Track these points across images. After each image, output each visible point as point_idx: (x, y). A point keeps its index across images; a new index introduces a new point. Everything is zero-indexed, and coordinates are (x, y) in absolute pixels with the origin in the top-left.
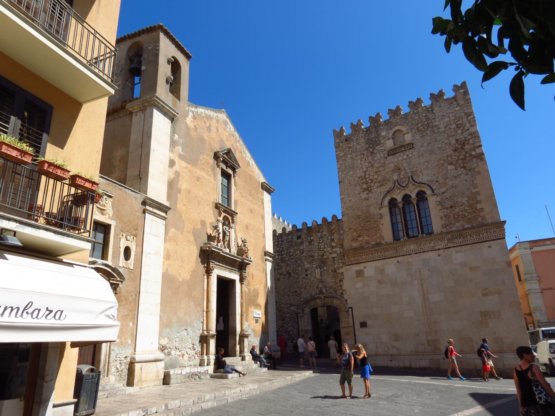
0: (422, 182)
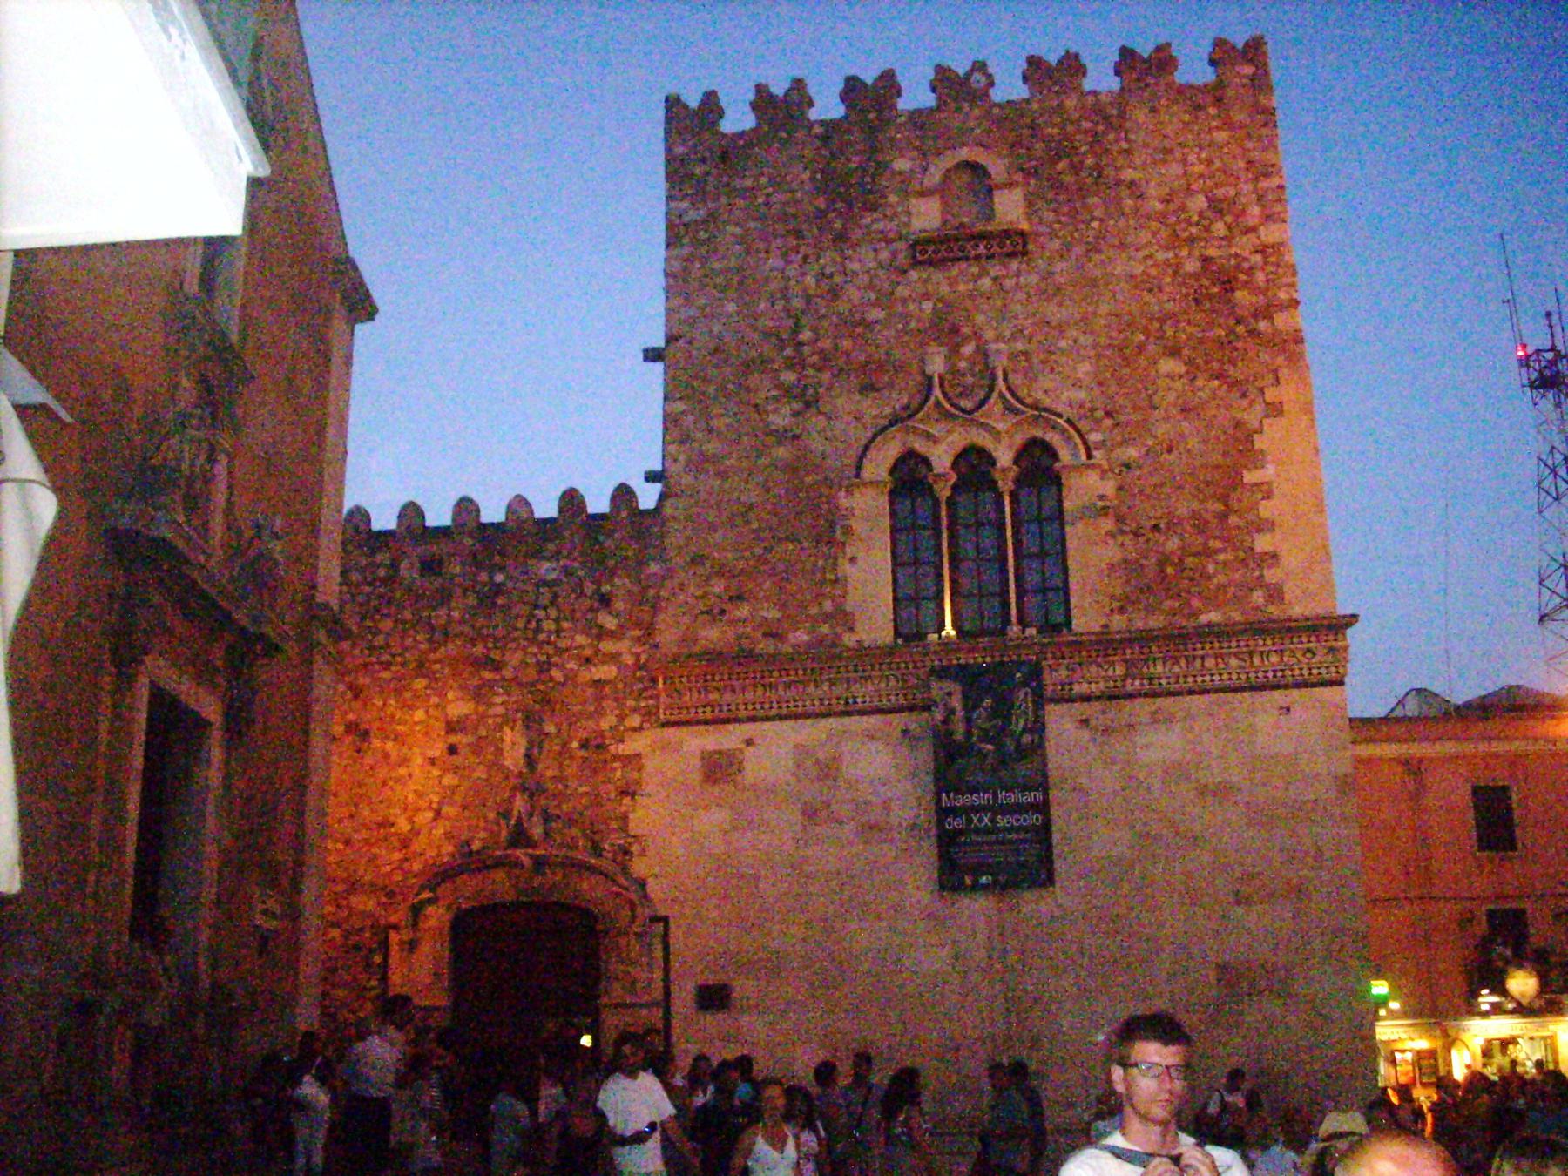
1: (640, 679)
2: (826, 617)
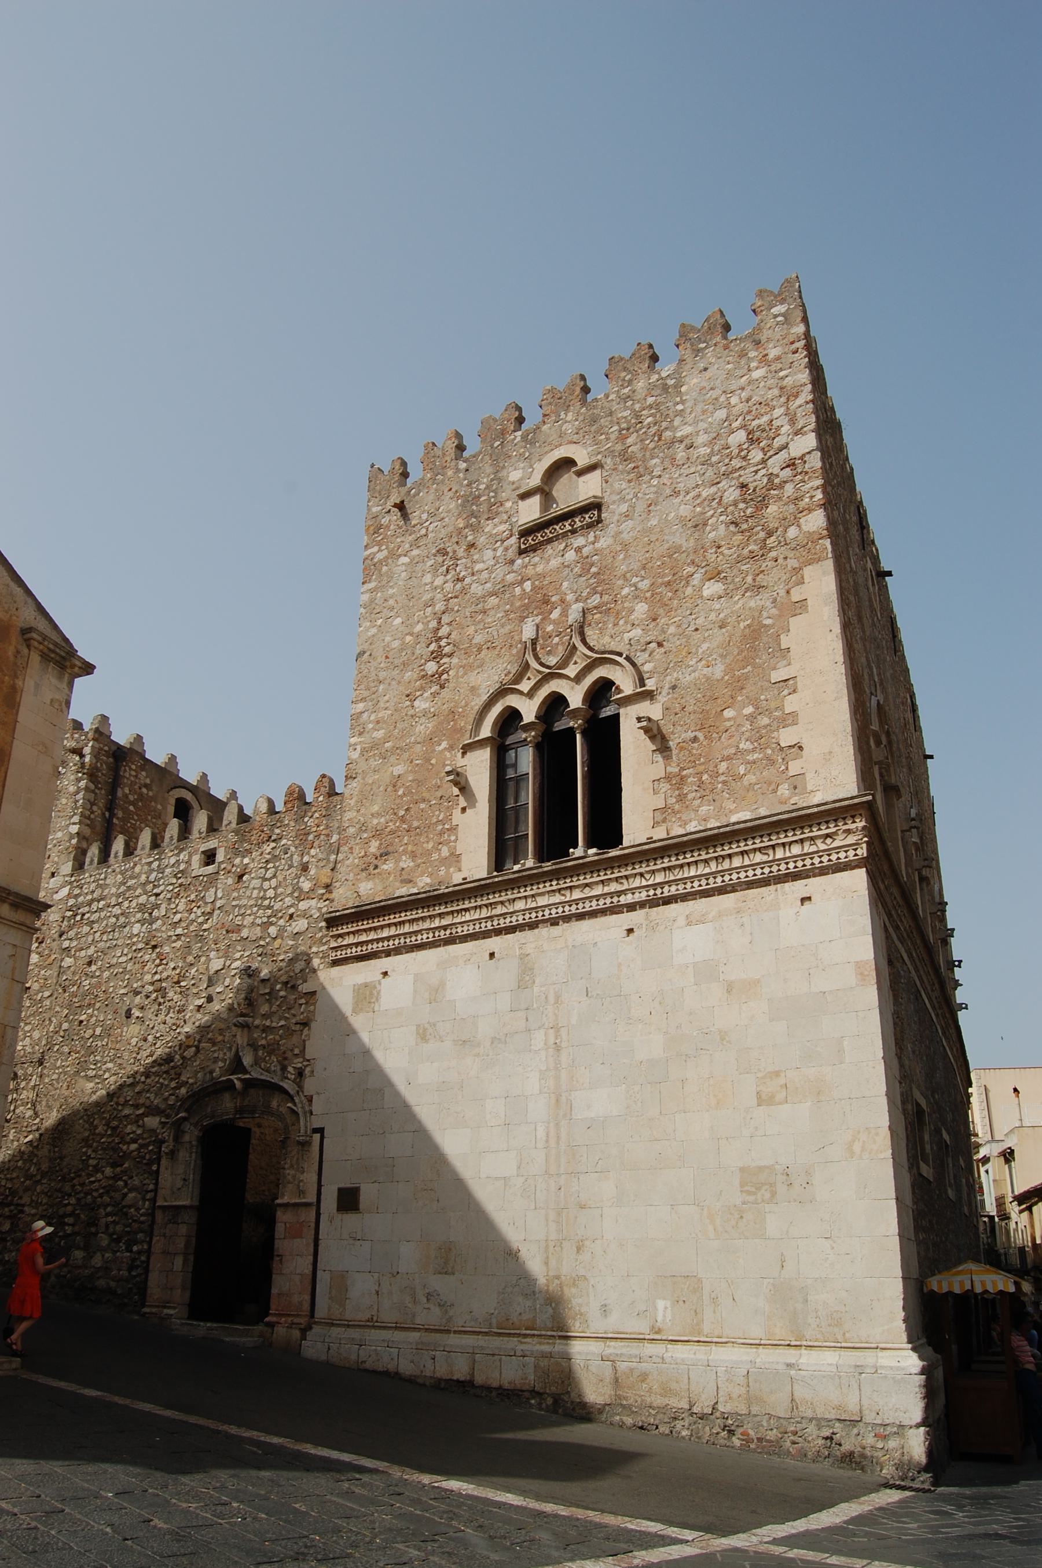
0: (613, 646)
2: (443, 861)
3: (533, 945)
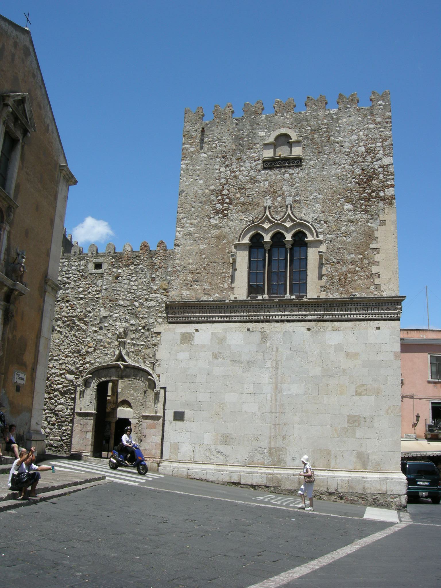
0: (305, 218)
1: (162, 307)
2: (225, 289)
3: (267, 328)
